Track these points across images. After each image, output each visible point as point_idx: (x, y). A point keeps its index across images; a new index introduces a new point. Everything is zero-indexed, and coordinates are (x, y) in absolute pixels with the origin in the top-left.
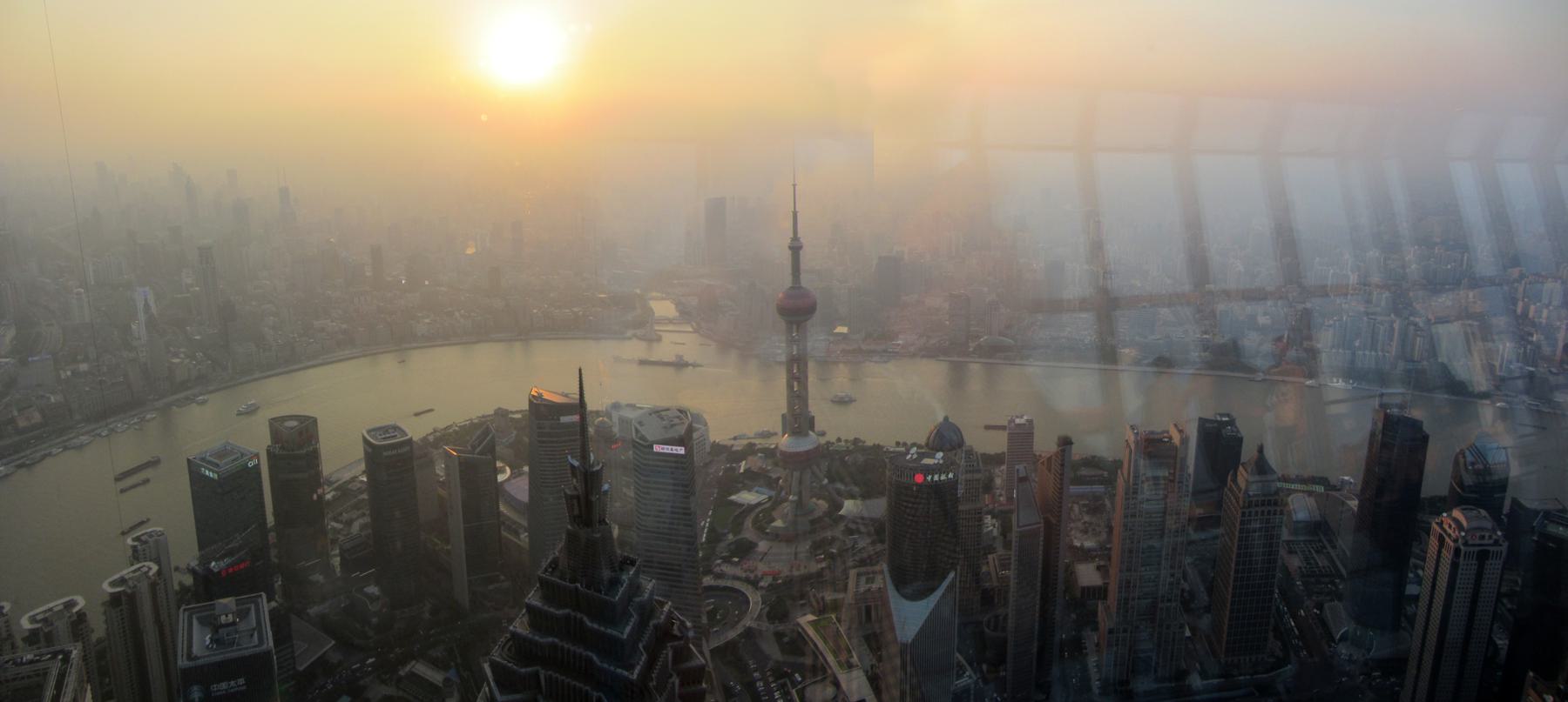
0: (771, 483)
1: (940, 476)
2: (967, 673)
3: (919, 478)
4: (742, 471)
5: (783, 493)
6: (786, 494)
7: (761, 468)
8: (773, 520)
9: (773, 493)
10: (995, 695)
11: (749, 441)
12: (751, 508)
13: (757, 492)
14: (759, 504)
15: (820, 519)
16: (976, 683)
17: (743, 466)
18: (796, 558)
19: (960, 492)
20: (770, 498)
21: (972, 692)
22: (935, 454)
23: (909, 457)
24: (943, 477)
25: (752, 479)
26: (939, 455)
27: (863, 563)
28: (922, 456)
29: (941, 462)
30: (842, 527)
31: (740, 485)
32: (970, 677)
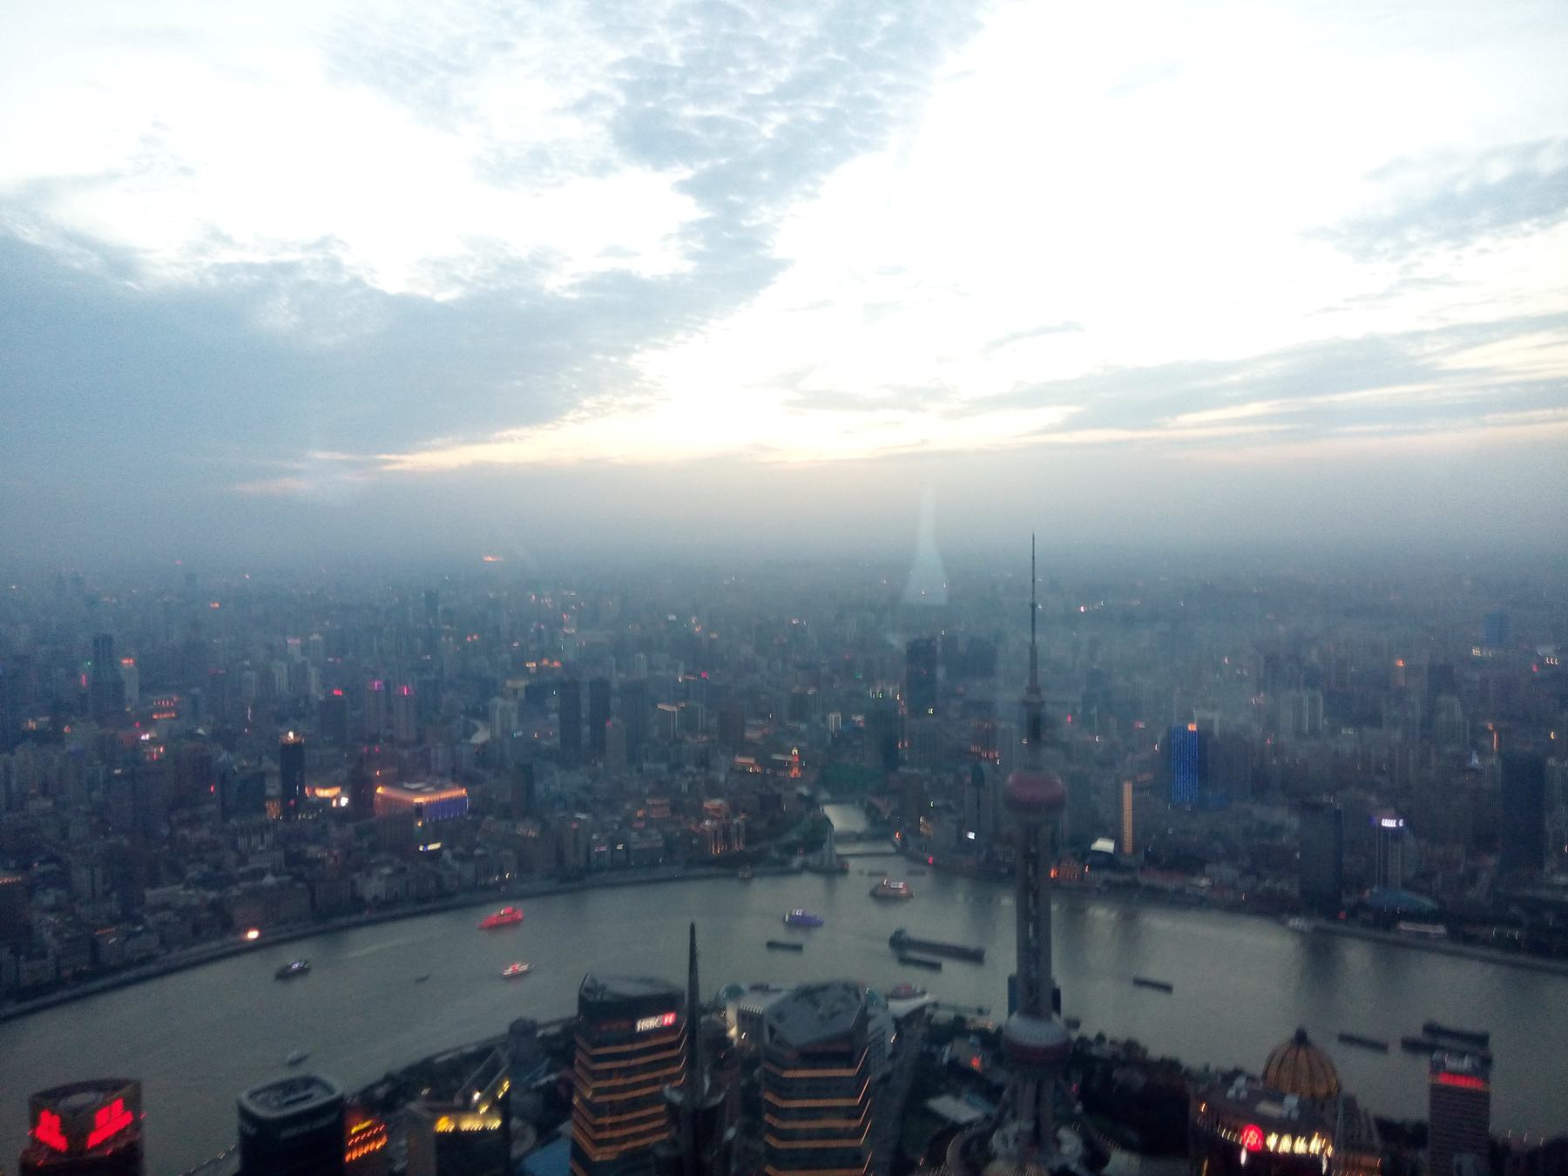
0: (991, 1092)
4: (945, 1060)
9: (994, 1111)
12: (955, 1128)
13: (968, 1101)
14: (970, 1124)
17: (947, 1053)
20: (988, 1118)
23: (1231, 1093)
24: (1300, 1147)
25: (959, 1078)
28: (1256, 1097)
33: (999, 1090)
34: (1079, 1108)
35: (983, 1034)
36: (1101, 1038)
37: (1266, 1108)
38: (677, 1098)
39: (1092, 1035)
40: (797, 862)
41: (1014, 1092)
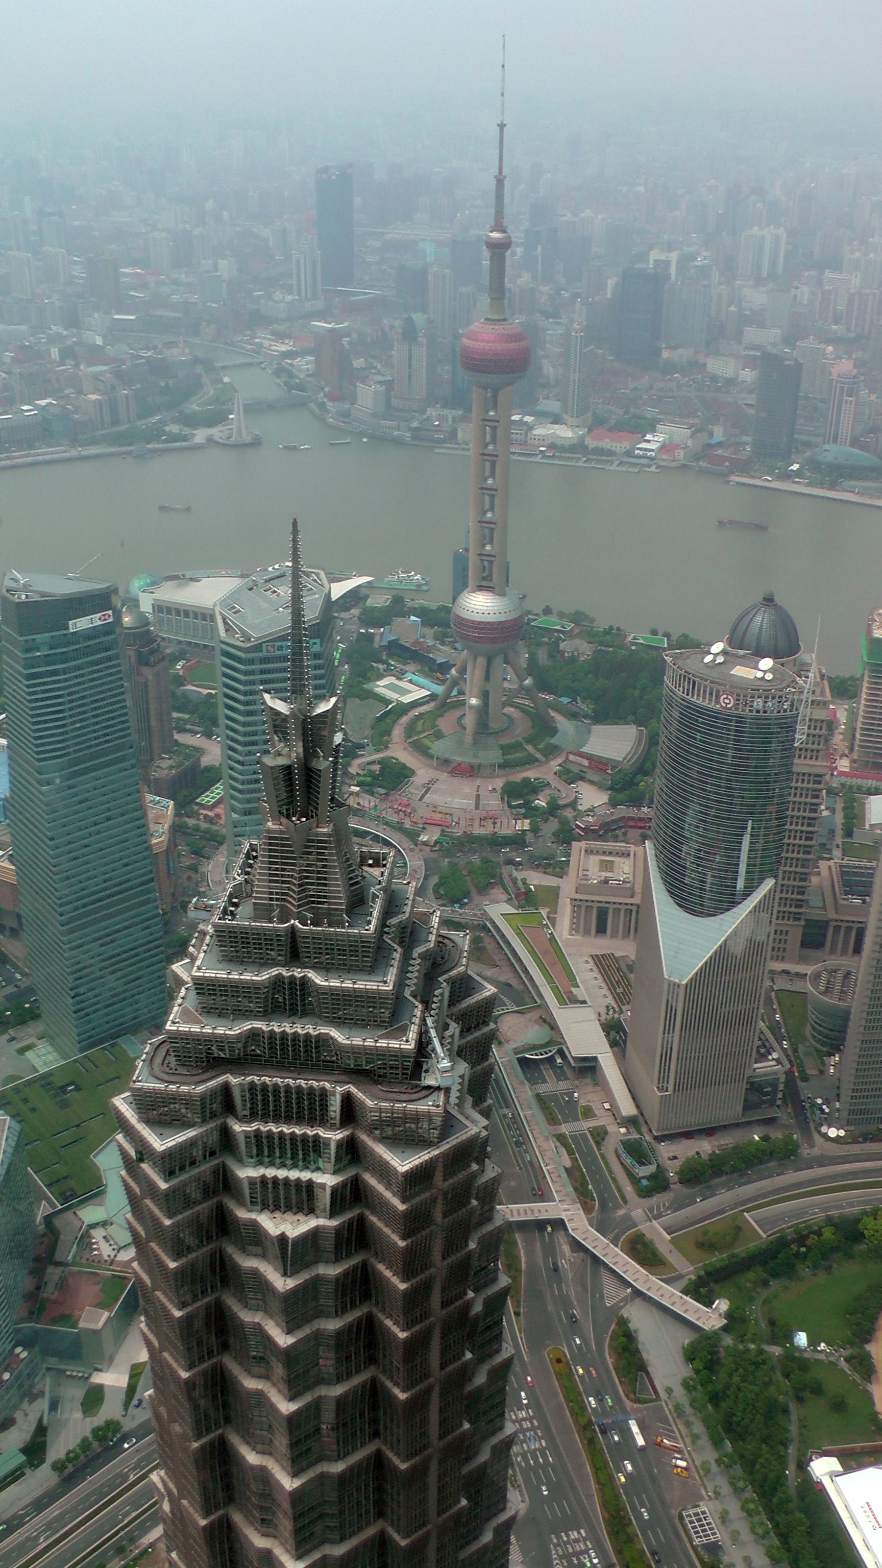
1: (766, 702)
2: (775, 1055)
3: (727, 702)
4: (385, 643)
5: (454, 693)
6: (461, 693)
7: (417, 643)
8: (439, 735)
9: (439, 689)
10: (819, 1101)
11: (395, 593)
12: (403, 709)
13: (410, 681)
14: (415, 704)
15: (516, 747)
16: (789, 1073)
18: (477, 807)
19: (800, 738)
20: (433, 697)
21: (781, 1087)
22: (758, 662)
23: (708, 659)
26: (766, 663)
27: (590, 833)
29: (769, 677)
30: (555, 764)
31: (381, 667)
32: (778, 1061)
33: (444, 668)
34: (528, 682)
35: (421, 612)
36: (548, 611)
37: (740, 671)
38: (282, 707)
39: (538, 608)
40: (200, 436)
41: (463, 671)
